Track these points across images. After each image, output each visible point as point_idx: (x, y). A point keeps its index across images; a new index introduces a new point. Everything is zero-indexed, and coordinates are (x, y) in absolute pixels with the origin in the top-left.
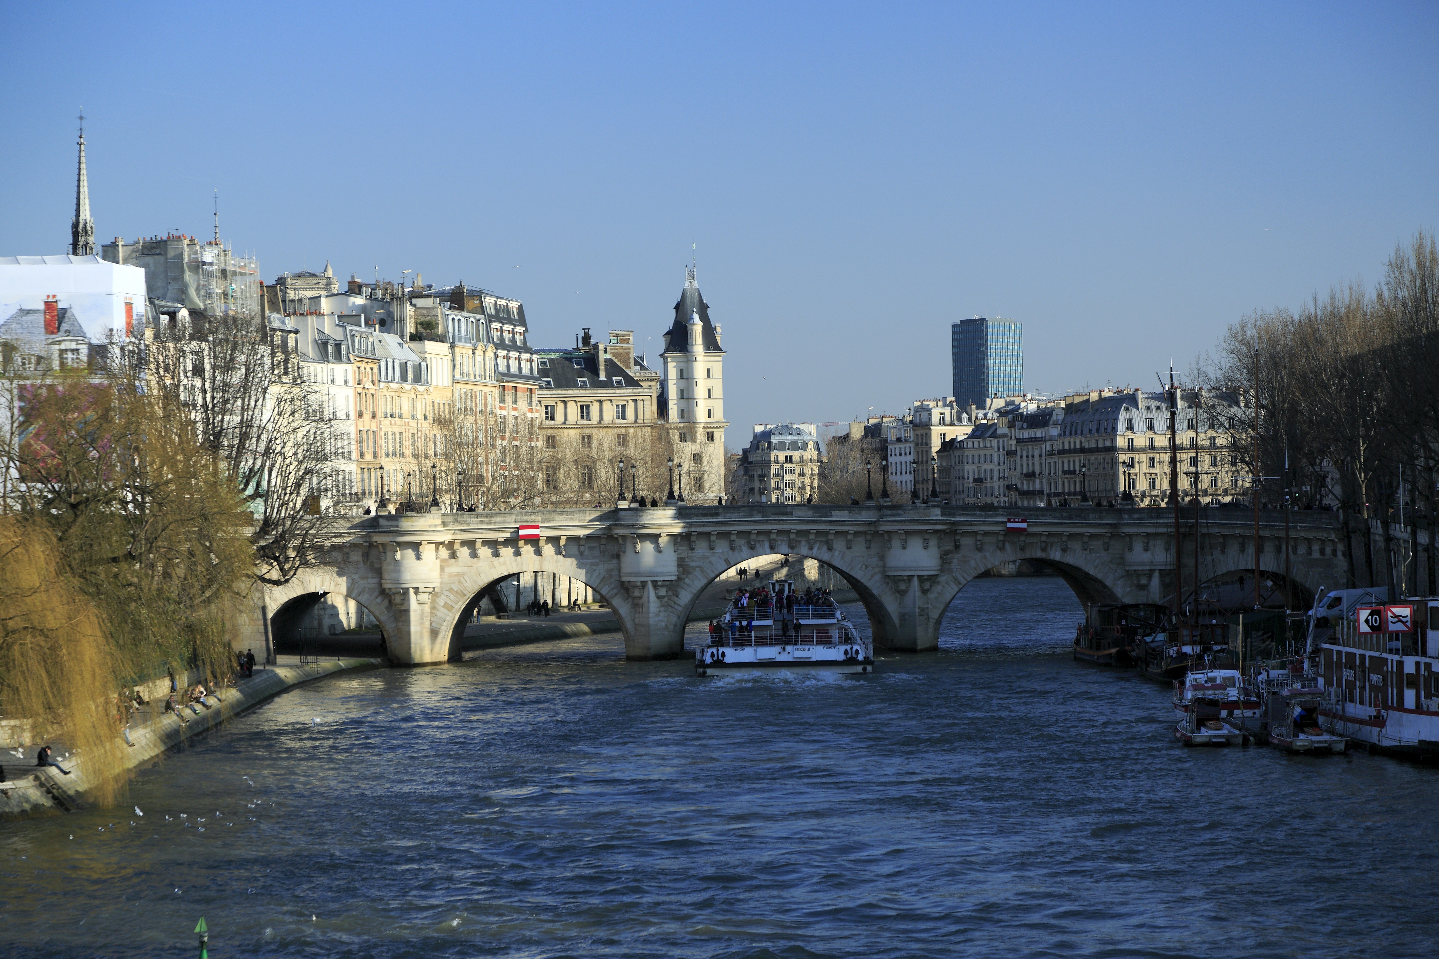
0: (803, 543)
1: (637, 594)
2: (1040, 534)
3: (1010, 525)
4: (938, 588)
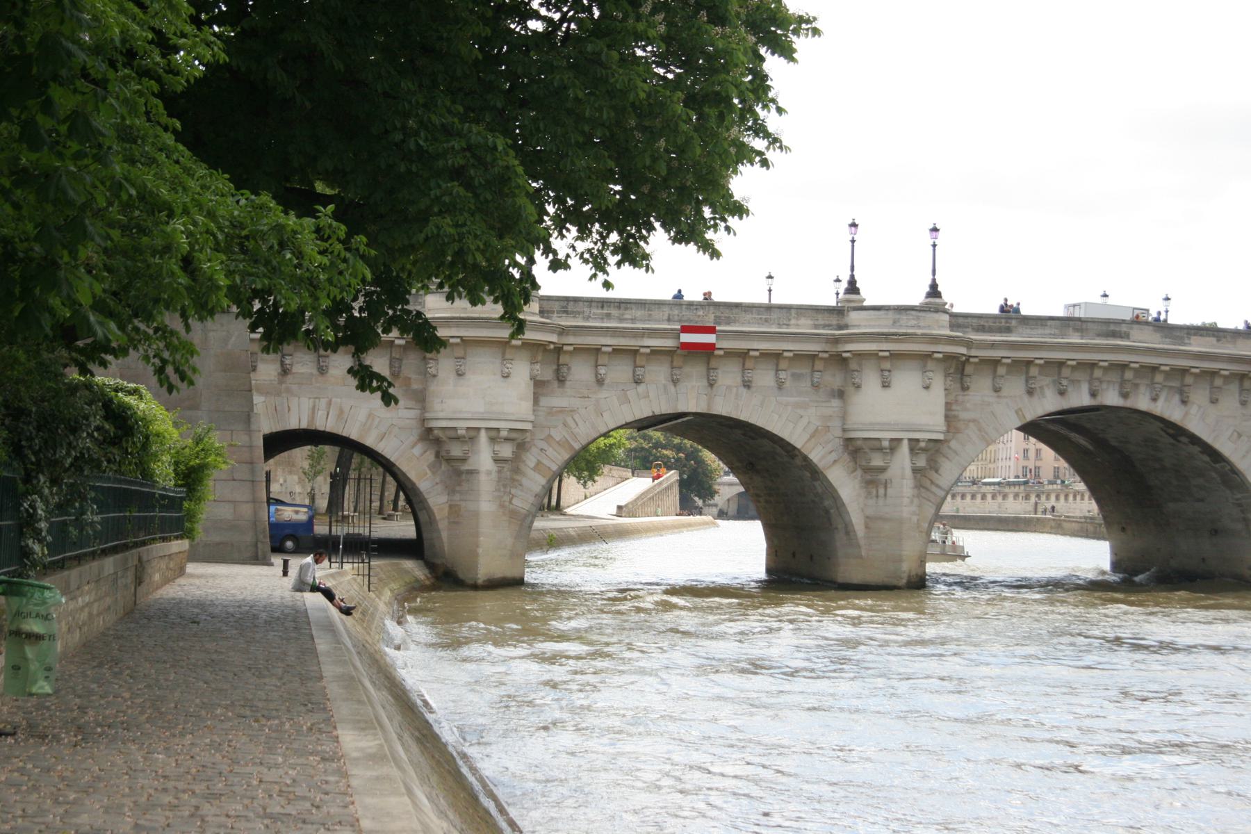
0: (1142, 389)
1: (877, 461)
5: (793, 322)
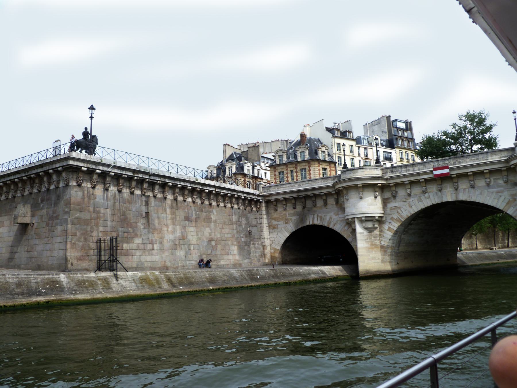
5: (490, 158)
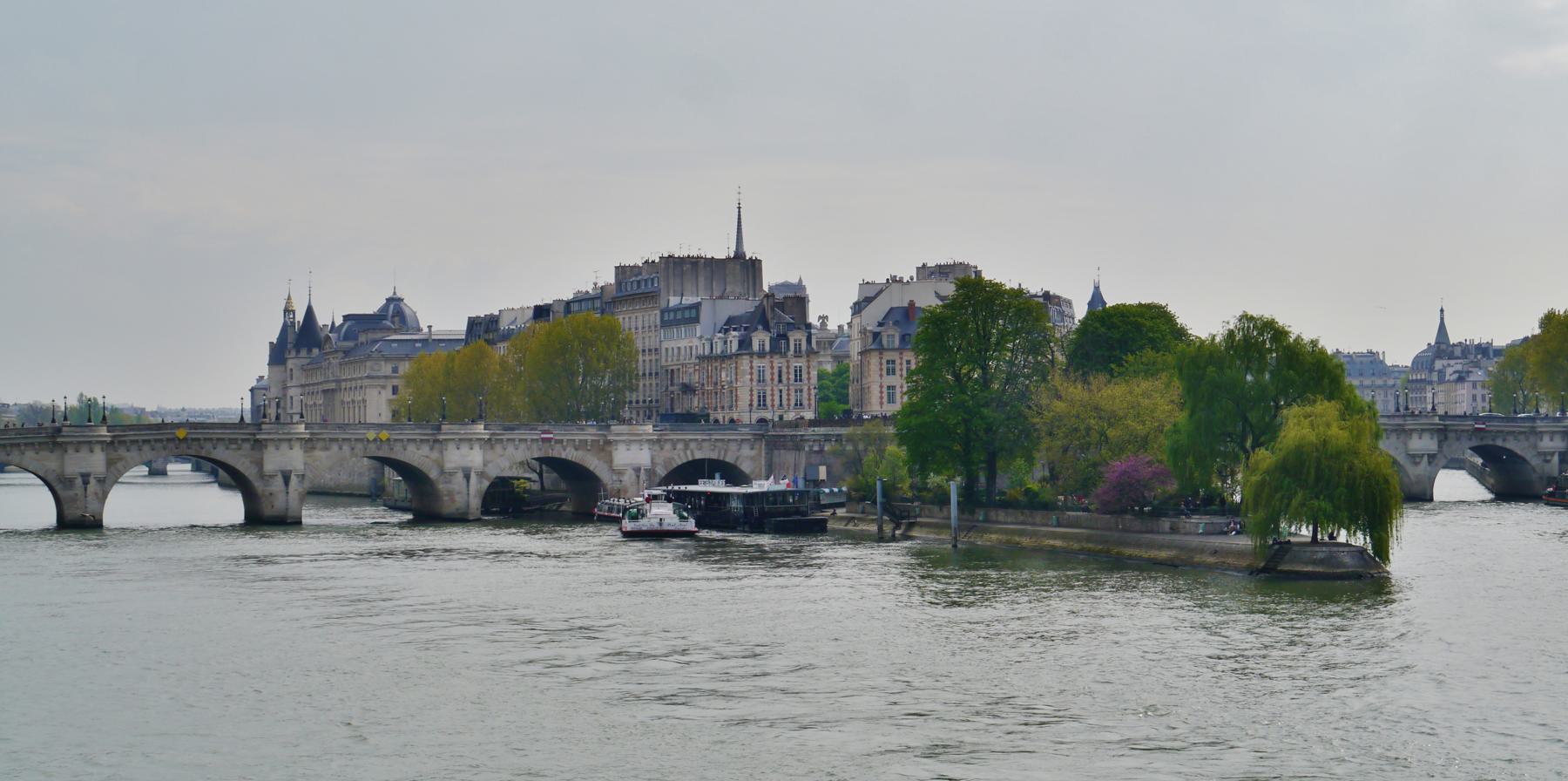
2: (1492, 431)
3: (1476, 426)
4: (1436, 461)
